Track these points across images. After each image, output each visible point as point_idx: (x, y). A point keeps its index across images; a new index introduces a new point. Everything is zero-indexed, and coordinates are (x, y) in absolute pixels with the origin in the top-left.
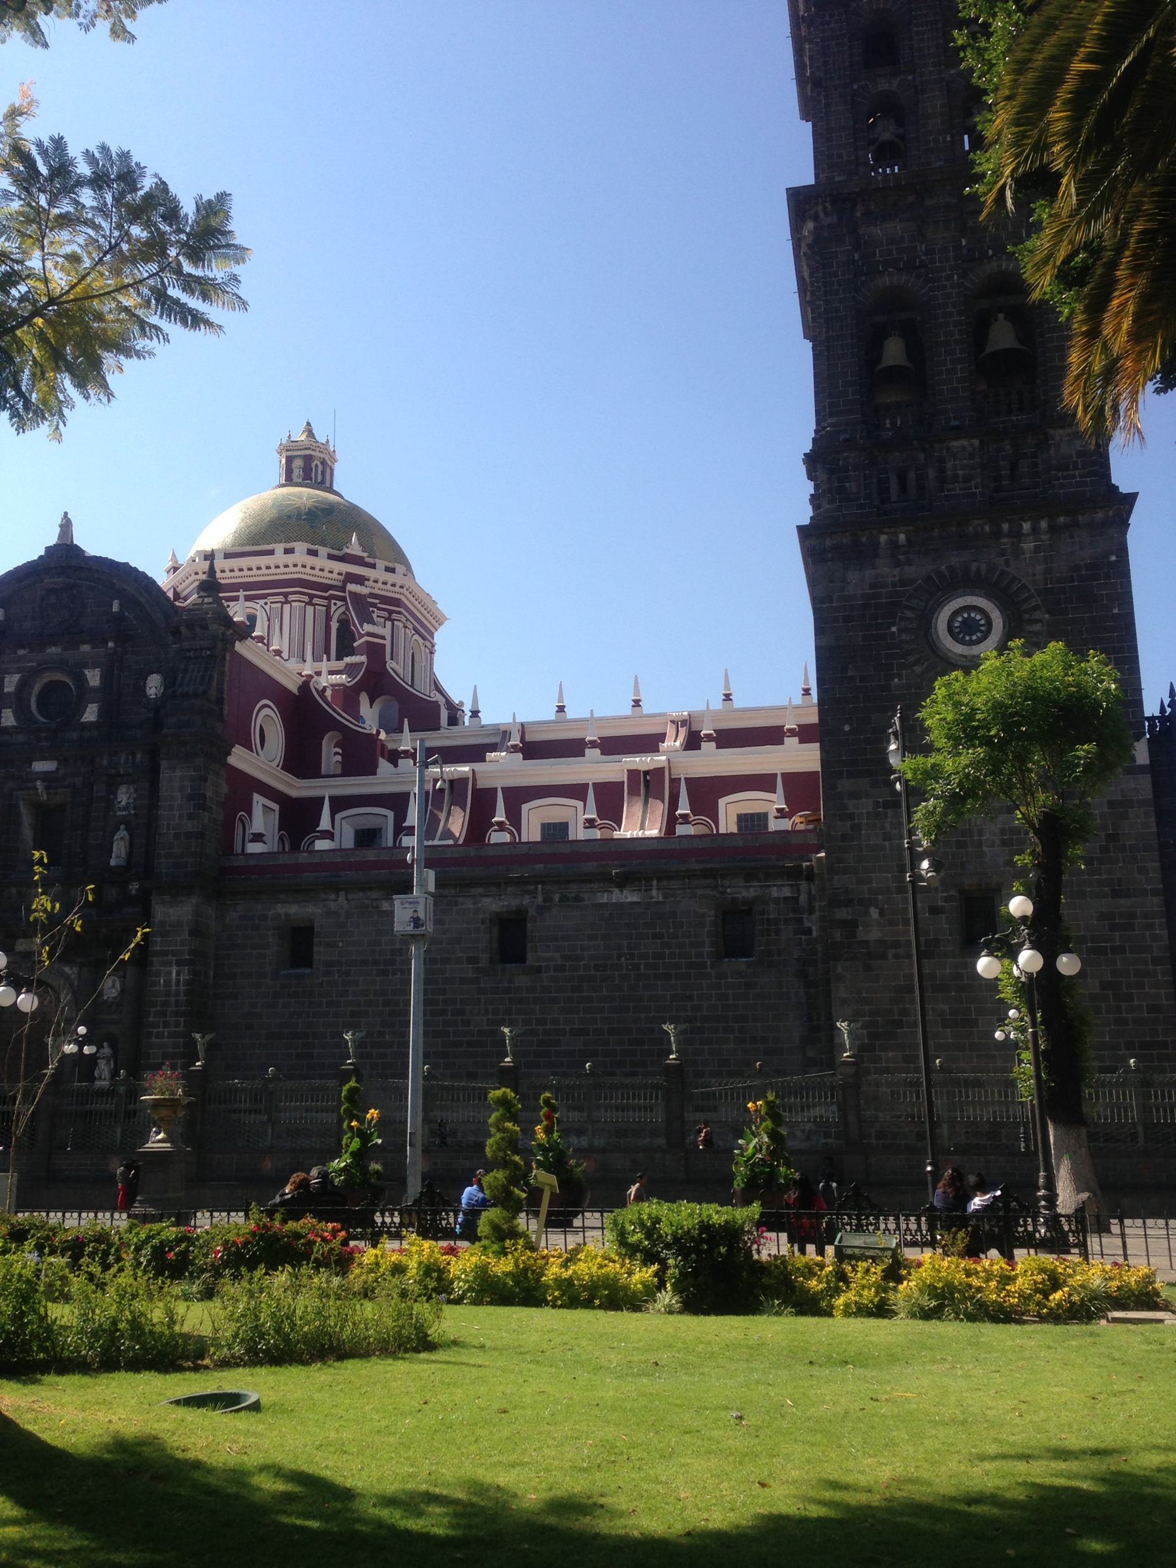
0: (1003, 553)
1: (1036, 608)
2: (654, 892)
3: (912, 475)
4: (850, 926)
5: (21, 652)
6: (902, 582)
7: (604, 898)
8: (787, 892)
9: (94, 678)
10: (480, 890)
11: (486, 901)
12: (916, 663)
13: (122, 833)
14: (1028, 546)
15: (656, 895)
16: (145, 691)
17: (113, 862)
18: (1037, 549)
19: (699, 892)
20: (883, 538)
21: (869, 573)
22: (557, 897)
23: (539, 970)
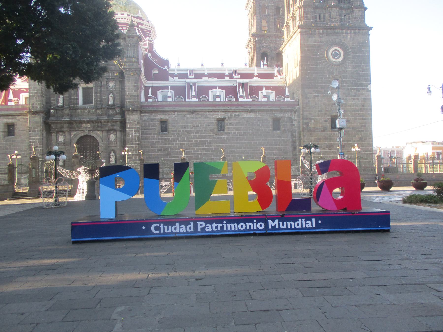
0: (343, 37)
1: (350, 52)
3: (322, 15)
4: (307, 124)
7: (245, 116)
8: (289, 115)
10: (213, 113)
11: (215, 115)
14: (349, 36)
18: (351, 38)
19: (269, 115)
21: (313, 39)
22: (233, 115)
23: (229, 133)
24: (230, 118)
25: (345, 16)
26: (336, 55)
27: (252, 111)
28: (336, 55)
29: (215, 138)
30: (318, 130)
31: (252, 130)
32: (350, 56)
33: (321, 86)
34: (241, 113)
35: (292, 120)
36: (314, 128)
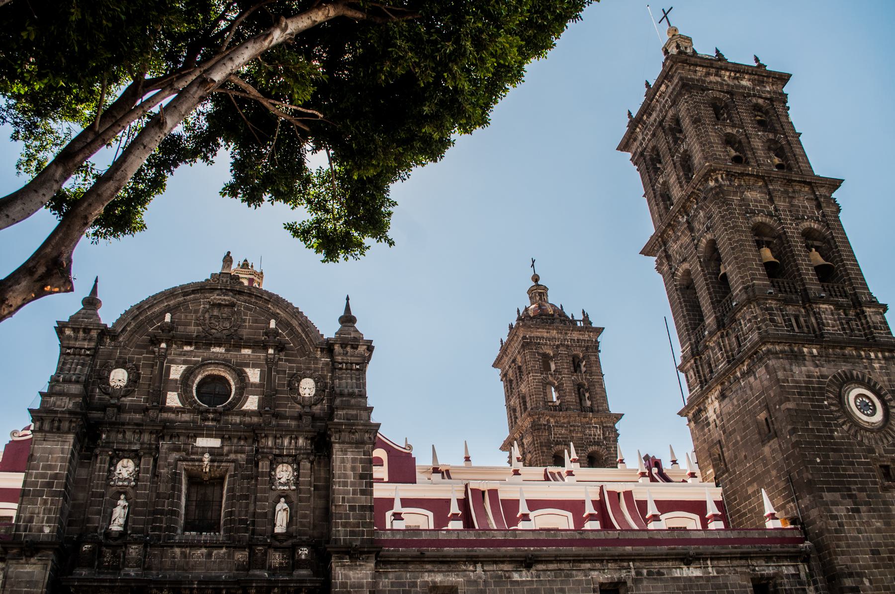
0: (866, 368)
2: (710, 569)
3: (802, 319)
5: (187, 348)
7: (677, 573)
8: (792, 571)
9: (254, 375)
10: (588, 565)
11: (594, 574)
12: (844, 423)
13: (282, 505)
15: (712, 572)
16: (298, 390)
17: (278, 530)
19: (739, 569)
22: (645, 571)
34: (665, 564)
35: (801, 583)
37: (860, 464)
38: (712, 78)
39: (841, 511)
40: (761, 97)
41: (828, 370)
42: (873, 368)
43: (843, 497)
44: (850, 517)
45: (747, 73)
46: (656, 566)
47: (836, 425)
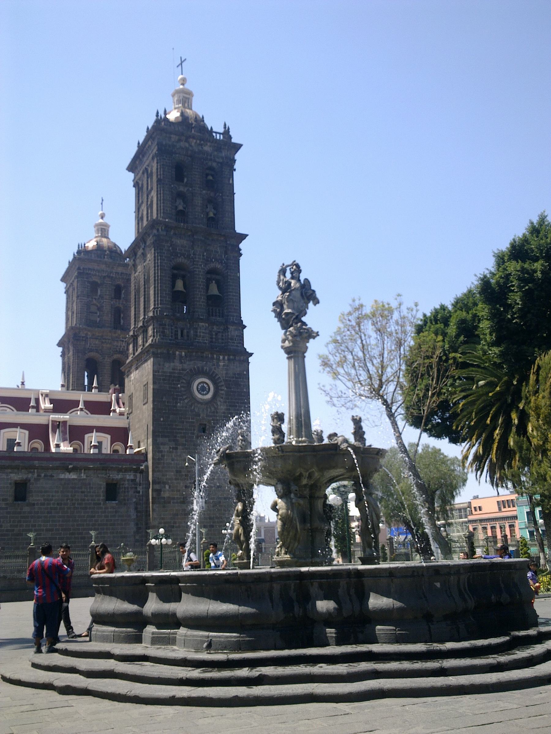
1: (222, 386)
2: (82, 475)
3: (185, 331)
6: (183, 370)
7: (62, 476)
8: (132, 477)
10: (10, 470)
12: (185, 399)
15: (83, 476)
19: (100, 475)
20: (177, 353)
21: (172, 364)
22: (43, 475)
23: (34, 504)
24: (37, 480)
25: (216, 334)
26: (203, 389)
27: (74, 469)
28: (203, 389)
29: (8, 513)
30: (175, 501)
31: (72, 500)
32: (222, 392)
33: (181, 433)
35: (136, 484)
36: (169, 497)
37: (187, 422)
38: (183, 144)
39: (166, 448)
40: (215, 161)
41: (188, 365)
42: (218, 366)
43: (169, 441)
44: (170, 452)
45: (209, 141)
46: (50, 473)
47: (180, 399)
